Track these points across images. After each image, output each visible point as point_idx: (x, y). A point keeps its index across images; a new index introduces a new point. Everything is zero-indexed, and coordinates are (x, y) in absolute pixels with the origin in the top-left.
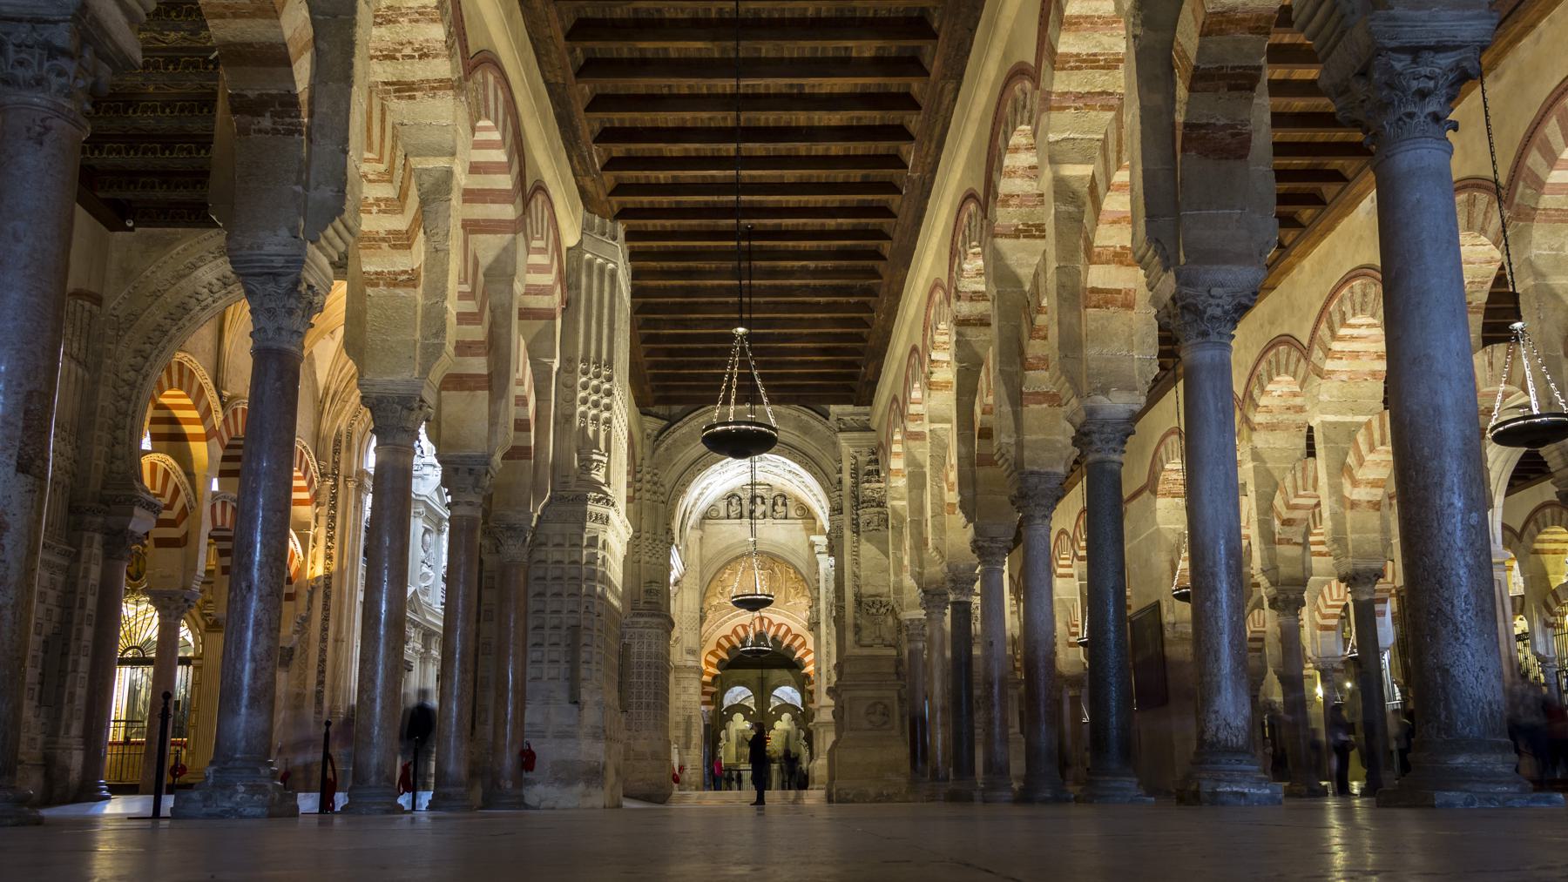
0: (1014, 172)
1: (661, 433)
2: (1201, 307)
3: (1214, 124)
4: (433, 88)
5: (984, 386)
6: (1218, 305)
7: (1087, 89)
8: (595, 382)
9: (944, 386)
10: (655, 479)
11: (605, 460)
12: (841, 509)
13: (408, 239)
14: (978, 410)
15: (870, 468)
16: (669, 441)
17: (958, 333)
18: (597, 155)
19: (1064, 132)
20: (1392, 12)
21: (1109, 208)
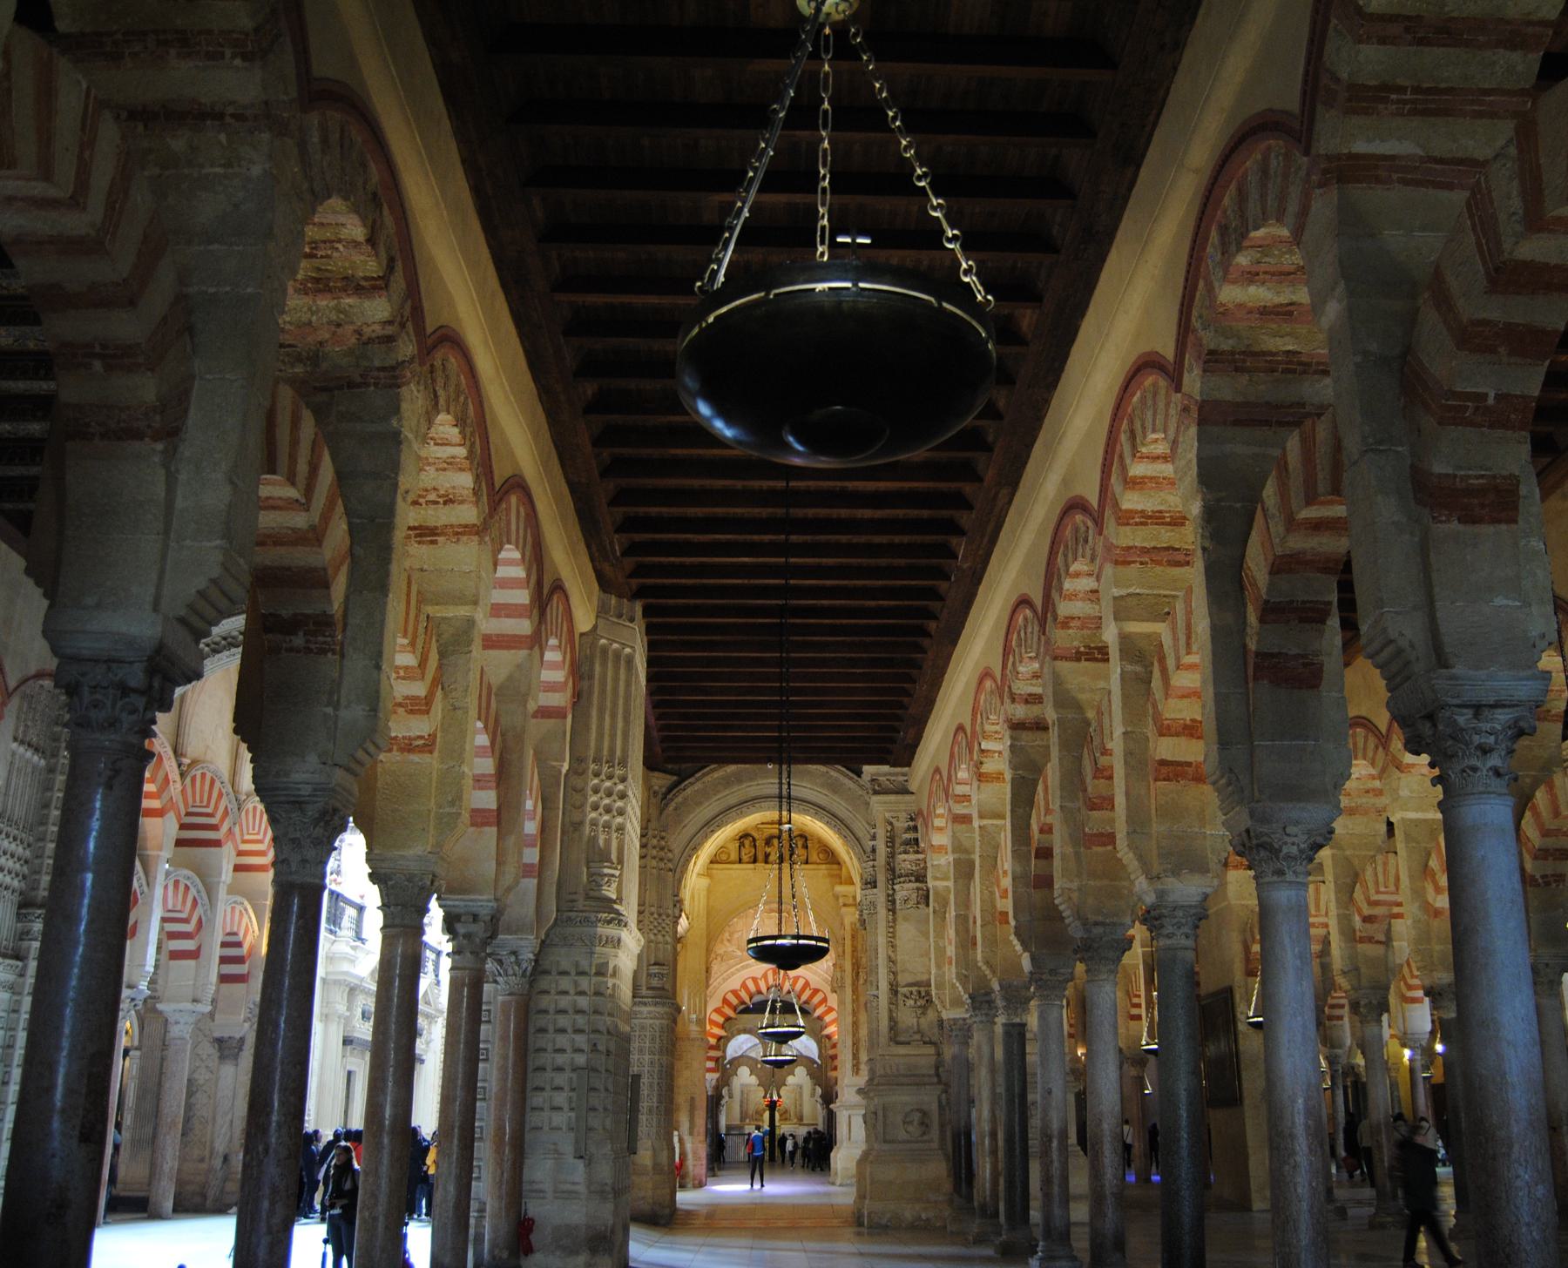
1: (670, 790)
2: (1276, 846)
4: (457, 533)
5: (1042, 803)
7: (1153, 544)
8: (608, 784)
9: (998, 777)
10: (663, 843)
11: (617, 873)
12: (875, 882)
13: (427, 704)
14: (1035, 827)
15: (908, 836)
16: (679, 799)
17: (1012, 738)
18: (617, 544)
19: (1130, 586)
20: (1454, 671)
21: (1178, 684)
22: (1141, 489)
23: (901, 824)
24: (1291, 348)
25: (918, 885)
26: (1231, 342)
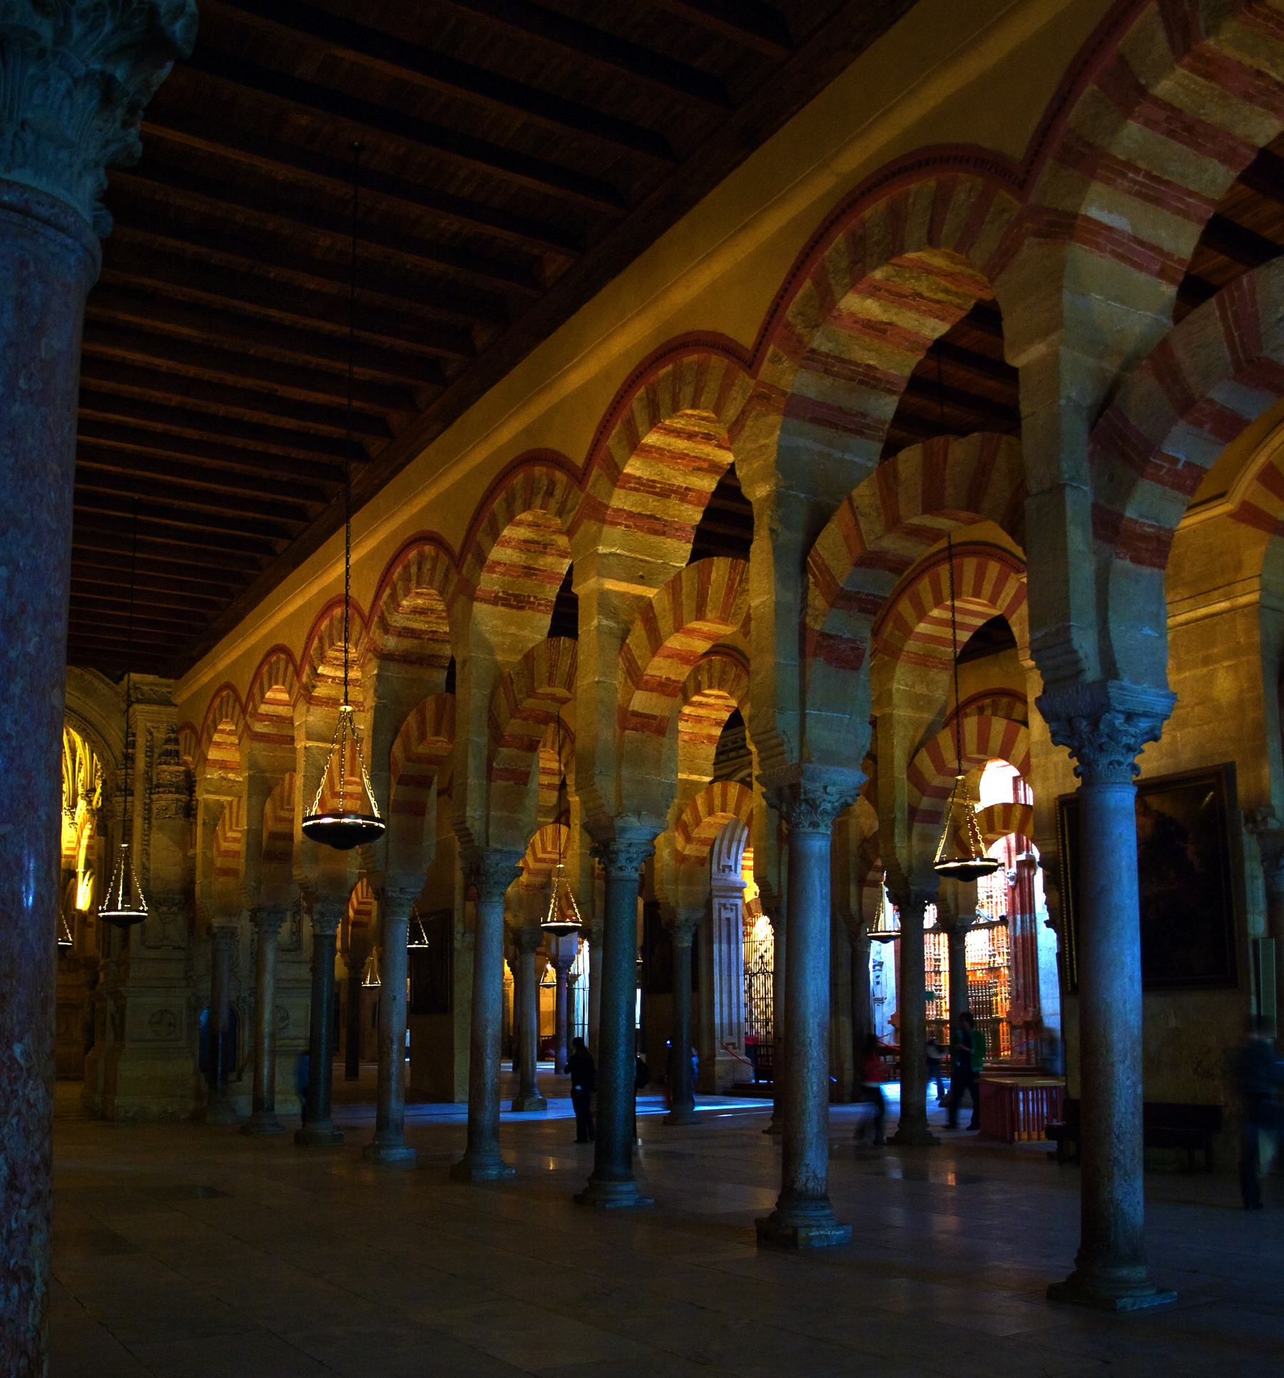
0: (508, 543)
3: (841, 637)
6: (830, 802)
7: (639, 510)
15: (169, 747)
19: (612, 546)
21: (669, 645)
22: (646, 457)
23: (160, 735)
24: (871, 362)
25: (177, 796)
26: (830, 345)
